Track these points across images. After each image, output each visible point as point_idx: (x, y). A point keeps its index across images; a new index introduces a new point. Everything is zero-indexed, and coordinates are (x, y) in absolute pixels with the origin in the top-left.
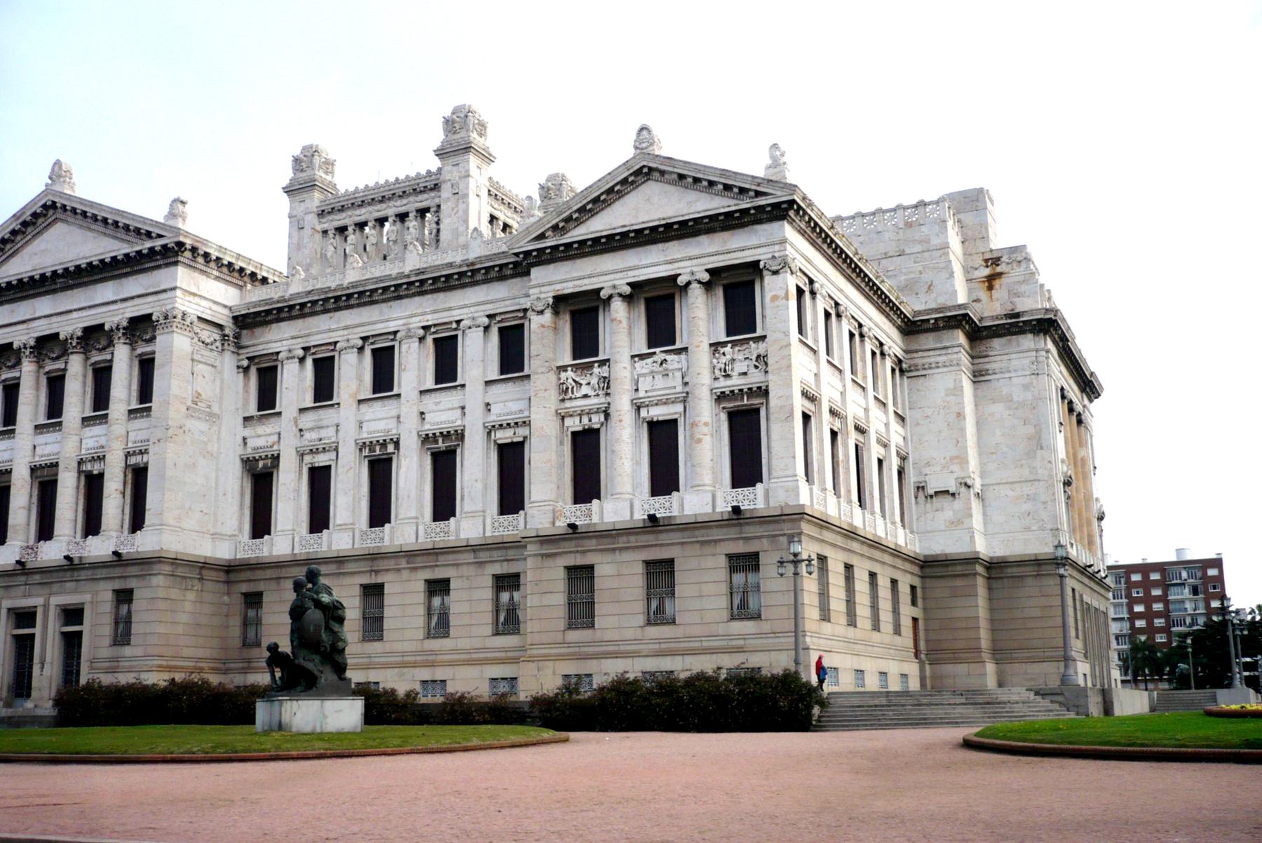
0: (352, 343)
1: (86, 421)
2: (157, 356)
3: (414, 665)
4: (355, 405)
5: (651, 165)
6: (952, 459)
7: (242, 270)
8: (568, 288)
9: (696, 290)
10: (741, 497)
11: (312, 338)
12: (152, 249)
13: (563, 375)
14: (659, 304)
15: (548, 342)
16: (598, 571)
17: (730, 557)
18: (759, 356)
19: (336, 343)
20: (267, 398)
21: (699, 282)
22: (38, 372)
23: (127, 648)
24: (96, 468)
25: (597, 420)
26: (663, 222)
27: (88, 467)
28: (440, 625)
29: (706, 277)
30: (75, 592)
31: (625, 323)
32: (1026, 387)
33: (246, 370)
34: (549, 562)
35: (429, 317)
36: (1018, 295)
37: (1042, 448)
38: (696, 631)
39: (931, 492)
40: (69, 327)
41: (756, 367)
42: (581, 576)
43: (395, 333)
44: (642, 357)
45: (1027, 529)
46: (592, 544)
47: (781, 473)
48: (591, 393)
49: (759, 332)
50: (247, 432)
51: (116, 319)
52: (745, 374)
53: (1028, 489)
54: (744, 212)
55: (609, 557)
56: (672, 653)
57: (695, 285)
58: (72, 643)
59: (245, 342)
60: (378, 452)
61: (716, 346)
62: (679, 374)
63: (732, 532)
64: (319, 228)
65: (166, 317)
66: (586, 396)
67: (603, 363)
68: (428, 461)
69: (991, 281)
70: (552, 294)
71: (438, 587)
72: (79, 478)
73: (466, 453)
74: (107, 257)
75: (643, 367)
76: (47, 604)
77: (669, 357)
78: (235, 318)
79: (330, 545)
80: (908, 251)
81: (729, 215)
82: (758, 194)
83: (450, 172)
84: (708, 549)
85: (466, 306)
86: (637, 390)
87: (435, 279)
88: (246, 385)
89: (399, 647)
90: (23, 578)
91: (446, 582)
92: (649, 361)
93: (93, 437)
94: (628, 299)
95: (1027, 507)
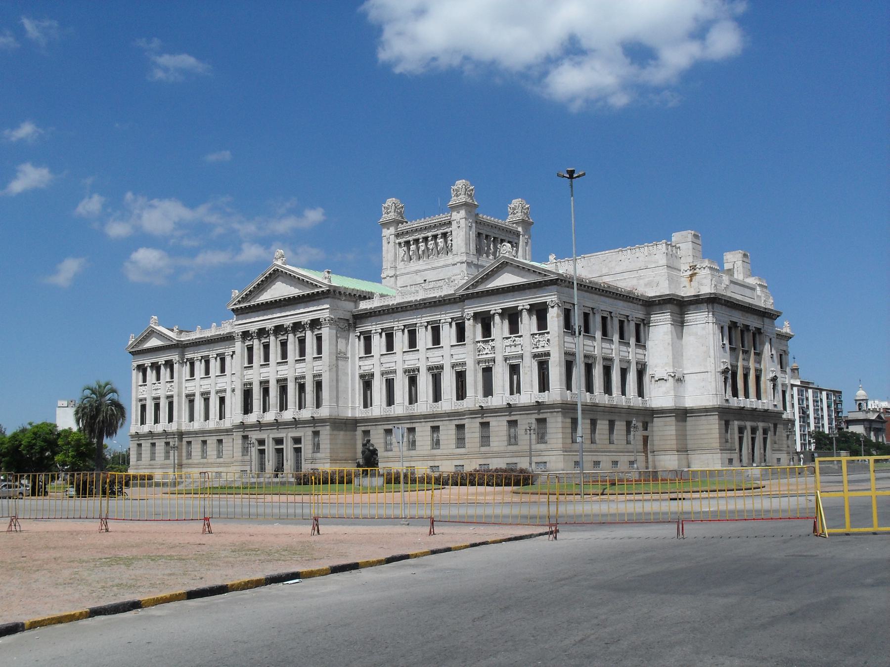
9: (525, 313)
14: (512, 317)
15: (474, 331)
20: (368, 349)
24: (302, 381)
28: (436, 444)
29: (528, 307)
32: (704, 329)
33: (359, 337)
44: (507, 338)
50: (361, 363)
55: (494, 419)
58: (298, 451)
61: (533, 335)
64: (397, 241)
67: (493, 340)
68: (430, 378)
71: (435, 429)
91: (438, 427)
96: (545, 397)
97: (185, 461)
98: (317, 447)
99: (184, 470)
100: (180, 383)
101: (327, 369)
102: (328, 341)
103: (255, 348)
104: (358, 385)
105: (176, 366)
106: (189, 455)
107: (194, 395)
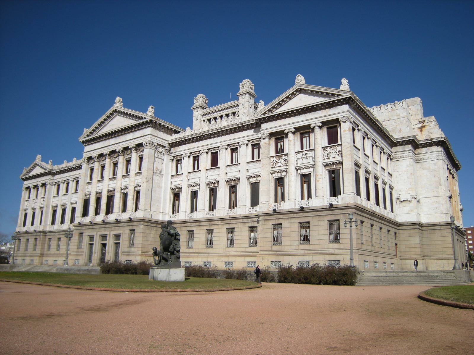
0: (205, 151)
1: (124, 176)
2: (144, 156)
3: (222, 256)
4: (205, 170)
5: (301, 88)
6: (409, 189)
7: (172, 129)
8: (274, 130)
10: (333, 200)
11: (192, 150)
12: (143, 122)
13: (272, 159)
16: (283, 226)
17: (329, 221)
18: (339, 151)
19: (200, 151)
21: (318, 126)
22: (110, 162)
23: (132, 248)
24: (126, 191)
25: (283, 174)
26: (305, 106)
27: (124, 191)
30: (118, 230)
31: (293, 141)
32: (435, 164)
34: (266, 223)
35: (229, 142)
36: (431, 133)
37: (441, 185)
38: (317, 247)
39: (402, 200)
40: (119, 148)
41: (338, 155)
42: (277, 226)
43: (218, 147)
44: (299, 152)
45: (436, 213)
46: (281, 216)
47: (347, 192)
48: (281, 165)
49: (339, 143)
50: (172, 180)
51: (132, 145)
52: (334, 157)
53: (436, 199)
54: (333, 102)
55: (287, 221)
56: (309, 255)
57: (317, 128)
59: (172, 151)
60: (212, 186)
61: (324, 148)
62: (311, 158)
63: (330, 212)
65: (147, 144)
66: (280, 166)
69: (421, 128)
70: (268, 132)
71: (231, 230)
72: (121, 194)
73: (240, 186)
74: (130, 125)
75: (299, 156)
76: (97, 234)
77: (308, 152)
78: (169, 144)
79: (196, 217)
80: (392, 119)
81: (328, 103)
82: (338, 95)
83: (242, 100)
84: (322, 218)
85: (241, 138)
86: (297, 164)
87: (231, 129)
88: (172, 166)
89: (218, 250)
90: (104, 226)
92: (302, 154)
93: (125, 182)
94: (294, 133)
95: (436, 205)
96: (338, 201)
97: (46, 252)
98: (132, 243)
99: (44, 258)
100: (49, 199)
101: (145, 180)
102: (147, 159)
103: (95, 168)
104: (169, 197)
105: (48, 187)
106: (49, 249)
107: (57, 206)
